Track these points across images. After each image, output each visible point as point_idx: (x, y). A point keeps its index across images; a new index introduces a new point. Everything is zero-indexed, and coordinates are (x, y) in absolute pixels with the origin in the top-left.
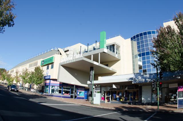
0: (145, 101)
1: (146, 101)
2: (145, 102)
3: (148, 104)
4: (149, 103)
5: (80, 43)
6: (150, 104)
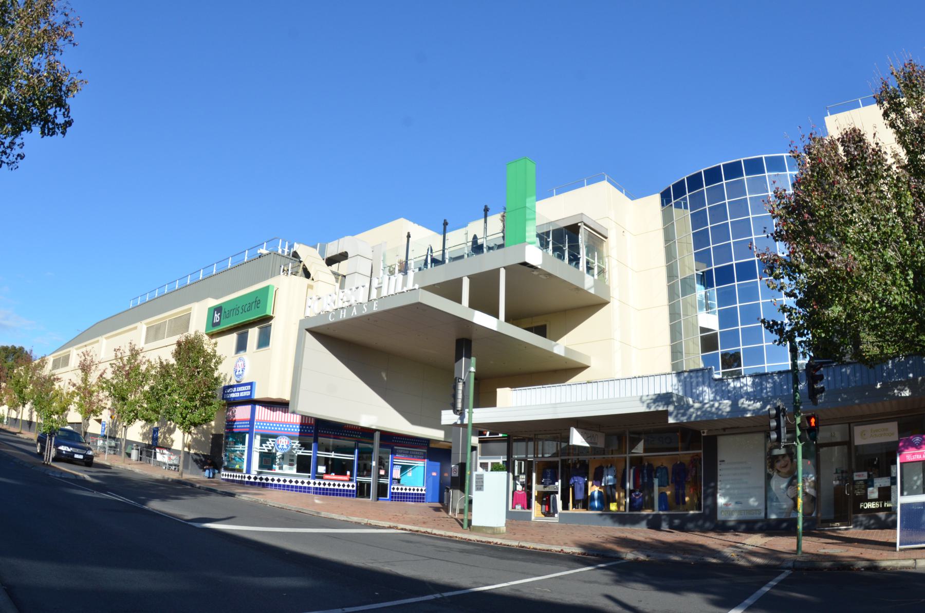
0: (734, 511)
1: (740, 511)
2: (734, 517)
3: (750, 527)
4: (755, 522)
5: (209, 298)
6: (760, 524)
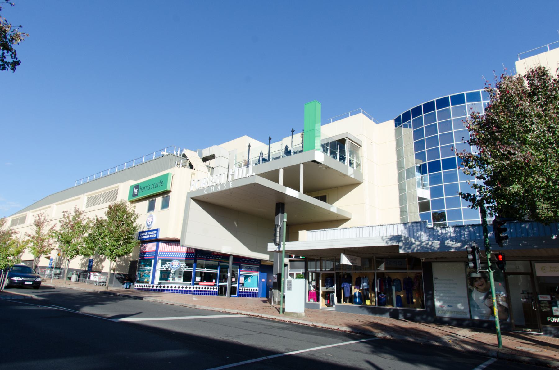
0: (447, 311)
1: (451, 312)
2: (448, 315)
3: (460, 323)
4: (463, 320)
6: (467, 322)
